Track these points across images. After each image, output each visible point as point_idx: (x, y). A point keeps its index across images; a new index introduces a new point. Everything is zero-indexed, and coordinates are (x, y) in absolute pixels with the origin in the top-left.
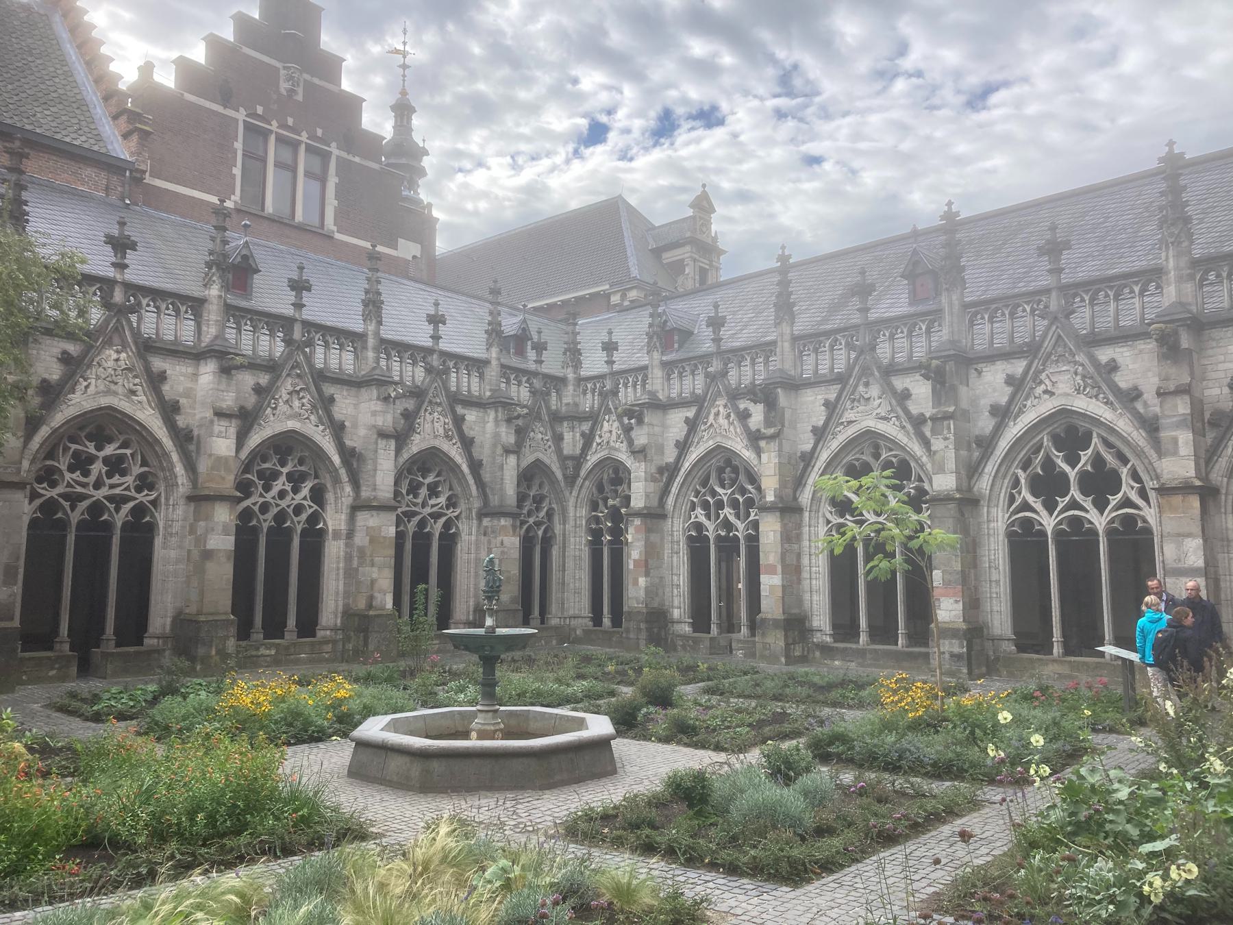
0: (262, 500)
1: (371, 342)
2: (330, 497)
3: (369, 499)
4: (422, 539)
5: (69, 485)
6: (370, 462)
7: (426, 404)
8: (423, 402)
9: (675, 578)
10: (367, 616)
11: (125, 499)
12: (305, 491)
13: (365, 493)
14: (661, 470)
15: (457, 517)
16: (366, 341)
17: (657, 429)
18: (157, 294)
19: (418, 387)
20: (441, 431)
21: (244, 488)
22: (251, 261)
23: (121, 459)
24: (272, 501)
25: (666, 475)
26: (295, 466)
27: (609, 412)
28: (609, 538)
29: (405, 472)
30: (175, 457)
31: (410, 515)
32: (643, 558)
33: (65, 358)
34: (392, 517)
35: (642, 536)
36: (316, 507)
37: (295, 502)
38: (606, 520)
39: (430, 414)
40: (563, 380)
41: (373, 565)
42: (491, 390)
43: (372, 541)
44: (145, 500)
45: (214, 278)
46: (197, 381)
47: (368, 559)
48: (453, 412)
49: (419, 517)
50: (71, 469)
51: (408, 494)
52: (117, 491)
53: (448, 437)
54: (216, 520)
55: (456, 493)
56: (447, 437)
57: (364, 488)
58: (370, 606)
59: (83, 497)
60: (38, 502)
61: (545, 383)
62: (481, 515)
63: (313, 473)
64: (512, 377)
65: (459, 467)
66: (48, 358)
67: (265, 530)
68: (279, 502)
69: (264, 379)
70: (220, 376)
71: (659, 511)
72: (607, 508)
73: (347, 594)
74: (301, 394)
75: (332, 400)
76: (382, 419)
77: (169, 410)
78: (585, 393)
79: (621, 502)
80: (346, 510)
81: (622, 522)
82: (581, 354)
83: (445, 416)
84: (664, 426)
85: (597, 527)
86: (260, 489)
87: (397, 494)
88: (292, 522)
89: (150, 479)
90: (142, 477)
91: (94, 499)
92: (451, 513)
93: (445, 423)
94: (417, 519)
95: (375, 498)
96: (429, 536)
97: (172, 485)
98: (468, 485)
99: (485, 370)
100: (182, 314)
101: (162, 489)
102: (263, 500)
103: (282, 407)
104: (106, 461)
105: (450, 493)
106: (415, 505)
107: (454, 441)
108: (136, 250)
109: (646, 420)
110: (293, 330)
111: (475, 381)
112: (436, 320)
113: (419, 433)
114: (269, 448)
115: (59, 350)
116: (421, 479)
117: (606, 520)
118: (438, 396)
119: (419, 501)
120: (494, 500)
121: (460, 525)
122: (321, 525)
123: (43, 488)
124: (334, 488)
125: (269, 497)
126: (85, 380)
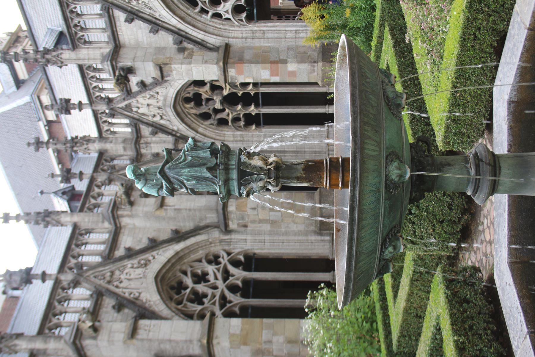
1: (39, 345)
3: (202, 346)
6: (162, 346)
7: (111, 287)
8: (108, 290)
9: (289, 35)
14: (182, 50)
15: (229, 254)
16: (38, 350)
17: (140, 54)
19: (91, 295)
20: (140, 271)
25: (186, 44)
27: (128, 108)
28: (252, 107)
29: (180, 307)
31: (224, 300)
32: (268, 65)
34: (221, 321)
35: (246, 67)
38: (236, 111)
39: (121, 282)
40: (101, 154)
41: (270, 342)
42: (103, 222)
43: (245, 344)
47: (264, 346)
48: (121, 259)
51: (202, 303)
55: (203, 256)
56: (146, 265)
61: (103, 170)
62: (227, 231)
64: (93, 201)
65: (177, 253)
71: (222, 51)
72: (223, 110)
78: (115, 133)
79: (217, 95)
81: (235, 94)
82: (77, 137)
83: (125, 267)
84: (137, 46)
85: (243, 119)
87: (201, 316)
92: (224, 260)
93: (132, 267)
94: (229, 295)
95: (200, 341)
96: (246, 282)
98: (197, 243)
99: (83, 228)
105: (204, 261)
106: (214, 296)
107: (151, 258)
109: (129, 64)
111: (93, 237)
113: (140, 293)
116: (188, 291)
117: (236, 111)
118: (103, 275)
119: (210, 292)
120: (212, 218)
121: (237, 251)
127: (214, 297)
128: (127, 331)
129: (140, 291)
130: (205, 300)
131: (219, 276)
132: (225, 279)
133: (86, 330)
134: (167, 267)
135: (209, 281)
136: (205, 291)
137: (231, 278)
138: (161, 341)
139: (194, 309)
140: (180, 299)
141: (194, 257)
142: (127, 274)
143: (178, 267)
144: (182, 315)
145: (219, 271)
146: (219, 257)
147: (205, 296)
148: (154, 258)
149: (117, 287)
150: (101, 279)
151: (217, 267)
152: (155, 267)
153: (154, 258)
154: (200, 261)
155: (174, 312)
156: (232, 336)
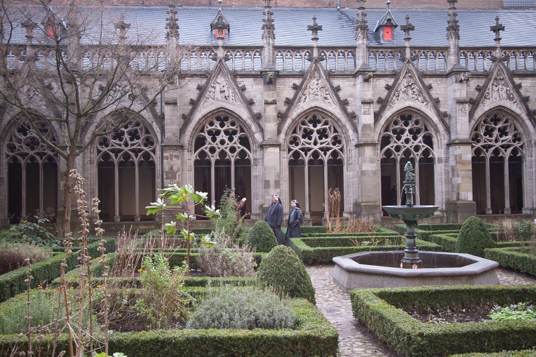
0: (395, 145)
2: (435, 140)
3: (455, 140)
4: (497, 160)
5: (303, 144)
6: (454, 119)
7: (491, 82)
10: (456, 204)
11: (328, 149)
12: (420, 138)
13: (453, 137)
15: (521, 147)
16: (450, 51)
18: (333, 49)
19: (486, 71)
20: (505, 95)
21: (385, 141)
22: (392, 22)
23: (325, 130)
24: (401, 145)
26: (413, 125)
29: (482, 122)
30: (348, 126)
31: (488, 147)
33: (295, 87)
36: (427, 146)
37: (414, 145)
39: (496, 86)
41: (458, 176)
43: (456, 163)
44: (337, 149)
45: (360, 35)
46: (356, 88)
47: (456, 172)
48: (513, 83)
49: (493, 148)
50: (304, 137)
52: (324, 145)
53: (510, 98)
54: (366, 156)
57: (452, 134)
58: (458, 199)
59: (310, 149)
60: (291, 152)
63: (423, 128)
65: (519, 116)
66: (288, 88)
67: (399, 160)
68: (405, 145)
69: (391, 82)
70: (364, 84)
73: (447, 193)
74: (413, 87)
75: (430, 87)
76: (459, 93)
77: (344, 104)
80: (444, 147)
83: (507, 86)
86: (395, 139)
88: (414, 155)
89: (339, 138)
90: (335, 138)
91: (314, 150)
92: (517, 145)
93: (507, 91)
94: (492, 149)
97: (348, 141)
98: (527, 127)
100: (346, 56)
101: (344, 143)
102: (397, 144)
103: (402, 95)
104: (318, 132)
105: (516, 132)
106: (490, 141)
107: (514, 101)
108: (321, 30)
110: (405, 53)
112: (497, 29)
113: (489, 99)
114: (398, 117)
115: (293, 84)
116: (493, 126)
119: (493, 138)
121: (524, 152)
122: (431, 156)
123: (293, 146)
124: (437, 135)
125: (399, 143)
126: (304, 95)
127: (490, 141)
128: (461, 99)
129: (491, 98)
130: (488, 136)
131: (504, 143)
132: (502, 146)
133: (460, 77)
134: (508, 111)
135: (501, 137)
136: (494, 136)
137: (503, 150)
138: (456, 118)
139: (481, 131)
140: (488, 122)
141: (518, 126)
142: (502, 88)
143: (510, 118)
144: (476, 125)
145: (508, 142)
146: (519, 141)
147: (491, 136)
148: (514, 102)
149: (493, 84)
150: (497, 74)
151: (511, 140)
152: (508, 104)
153: (514, 102)
154: (515, 129)
155: (478, 120)
156: (460, 156)
